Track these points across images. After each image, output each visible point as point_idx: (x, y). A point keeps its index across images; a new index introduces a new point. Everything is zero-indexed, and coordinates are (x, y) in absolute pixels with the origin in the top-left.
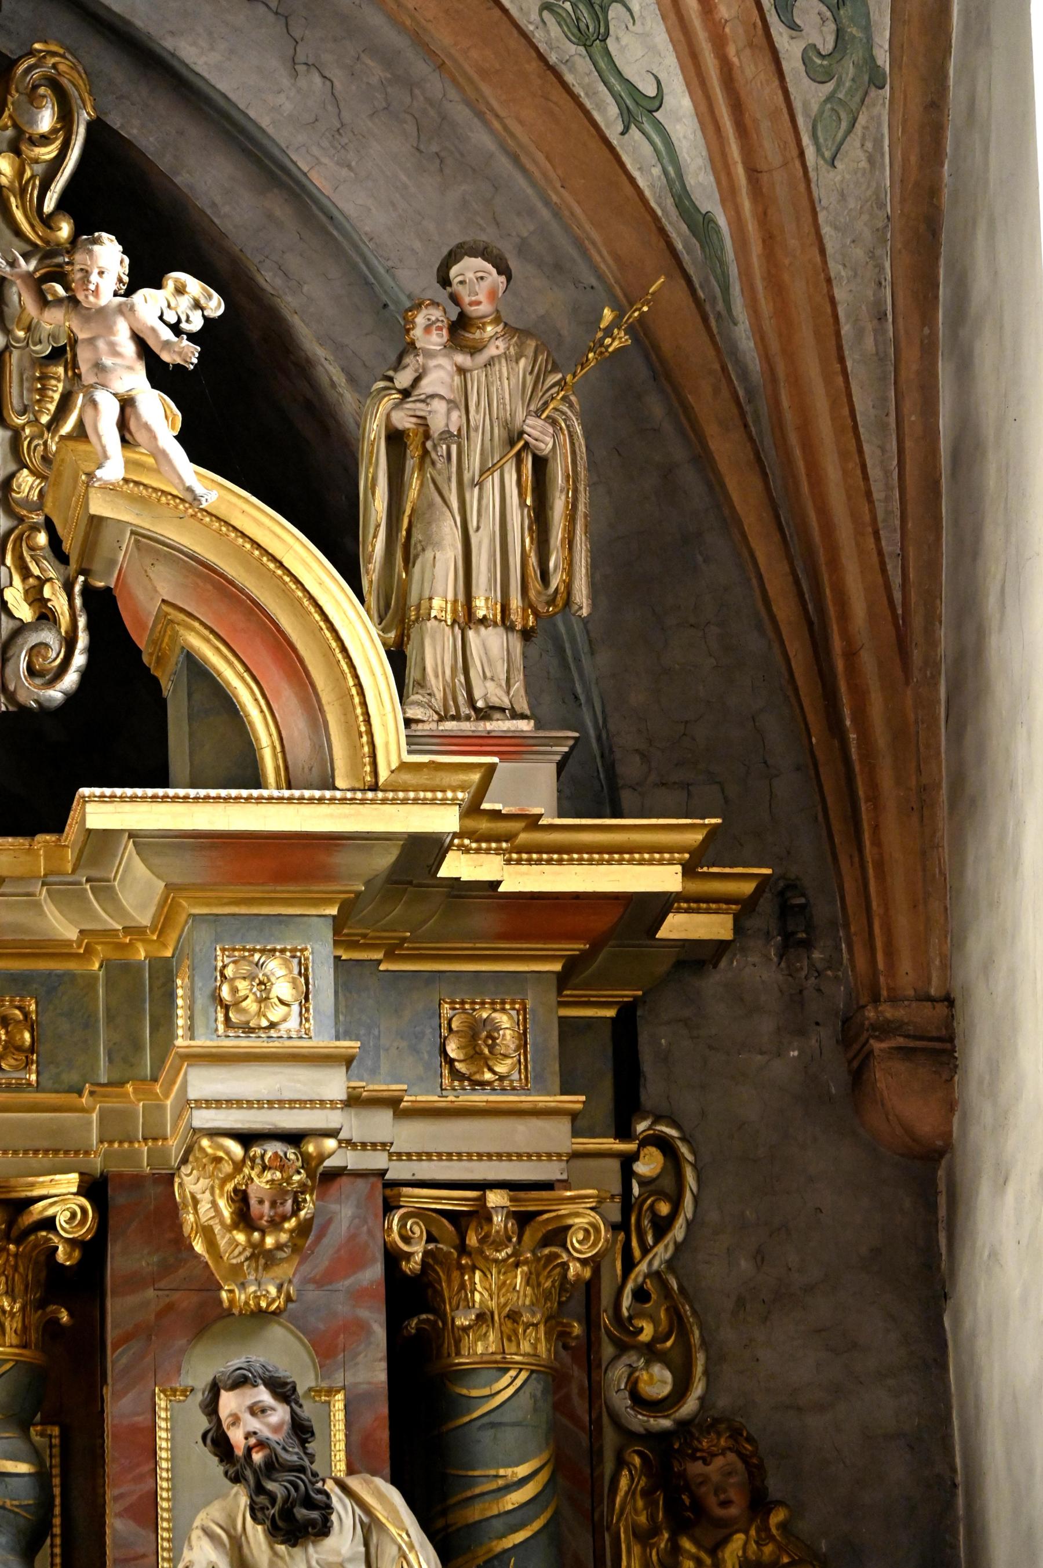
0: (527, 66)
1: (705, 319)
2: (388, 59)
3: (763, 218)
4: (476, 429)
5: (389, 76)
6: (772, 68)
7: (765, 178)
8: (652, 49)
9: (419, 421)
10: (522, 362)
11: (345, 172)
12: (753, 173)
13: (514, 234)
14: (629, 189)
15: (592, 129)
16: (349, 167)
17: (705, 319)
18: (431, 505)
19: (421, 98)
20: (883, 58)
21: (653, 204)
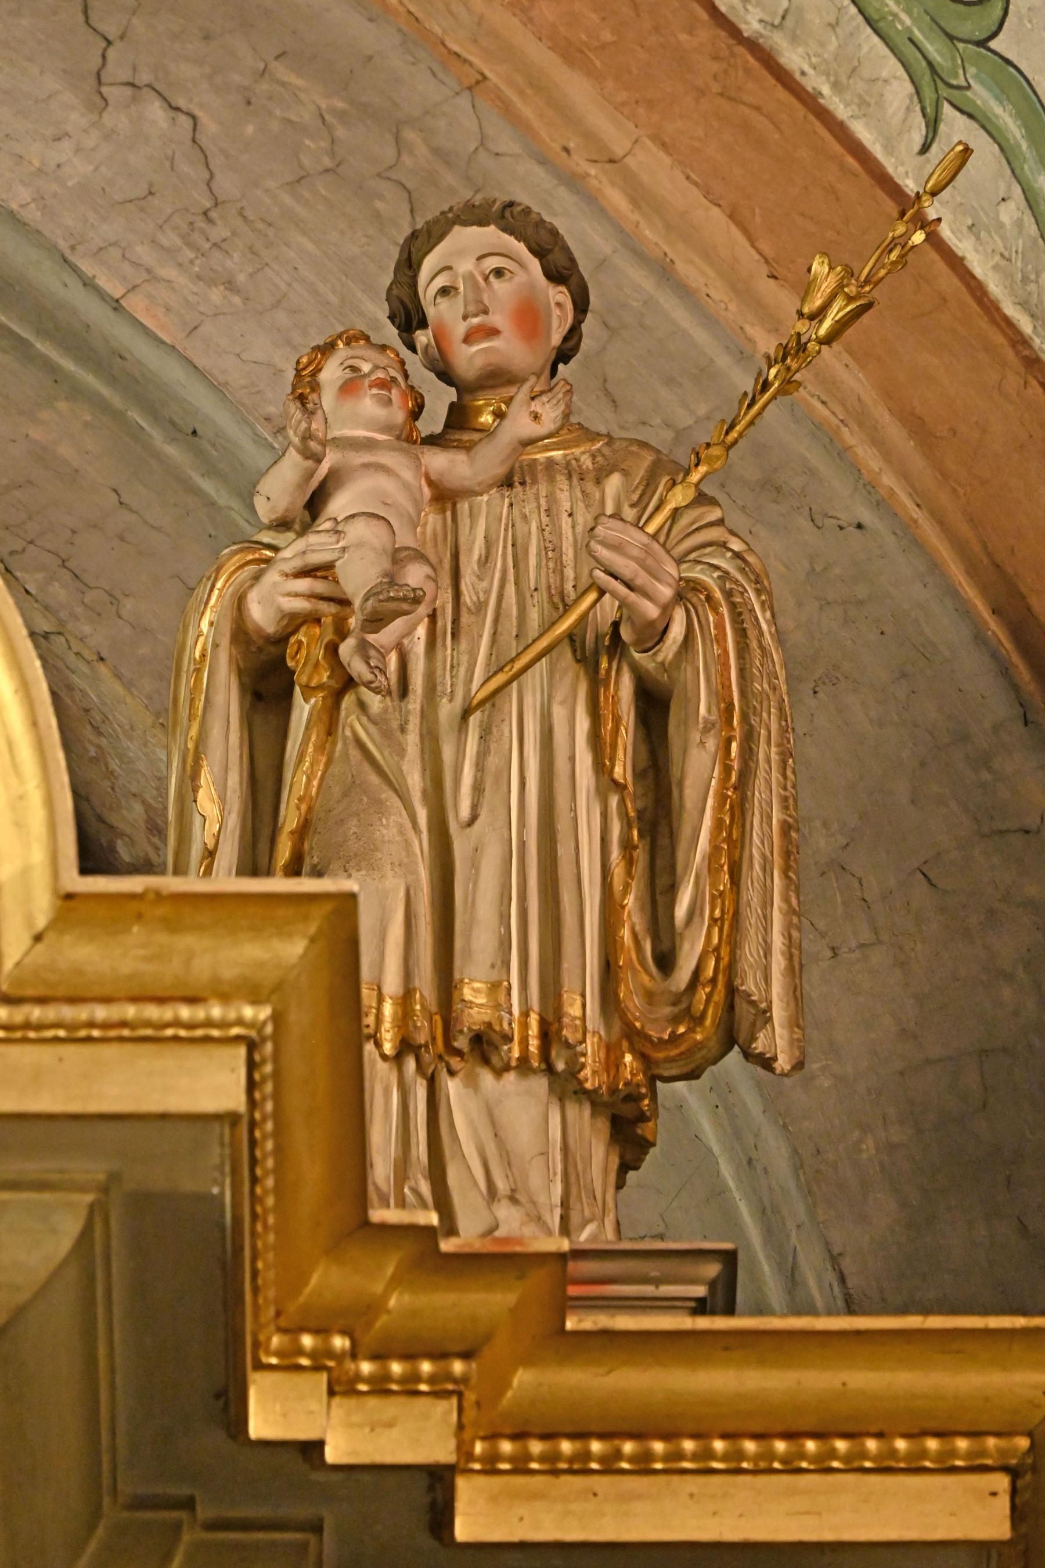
0: (683, 37)
4: (480, 607)
5: (340, 105)
9: (319, 586)
10: (614, 483)
11: (216, 295)
13: (657, 421)
14: (948, 281)
15: (850, 161)
16: (230, 285)
18: (353, 787)
19: (422, 150)
21: (1010, 310)
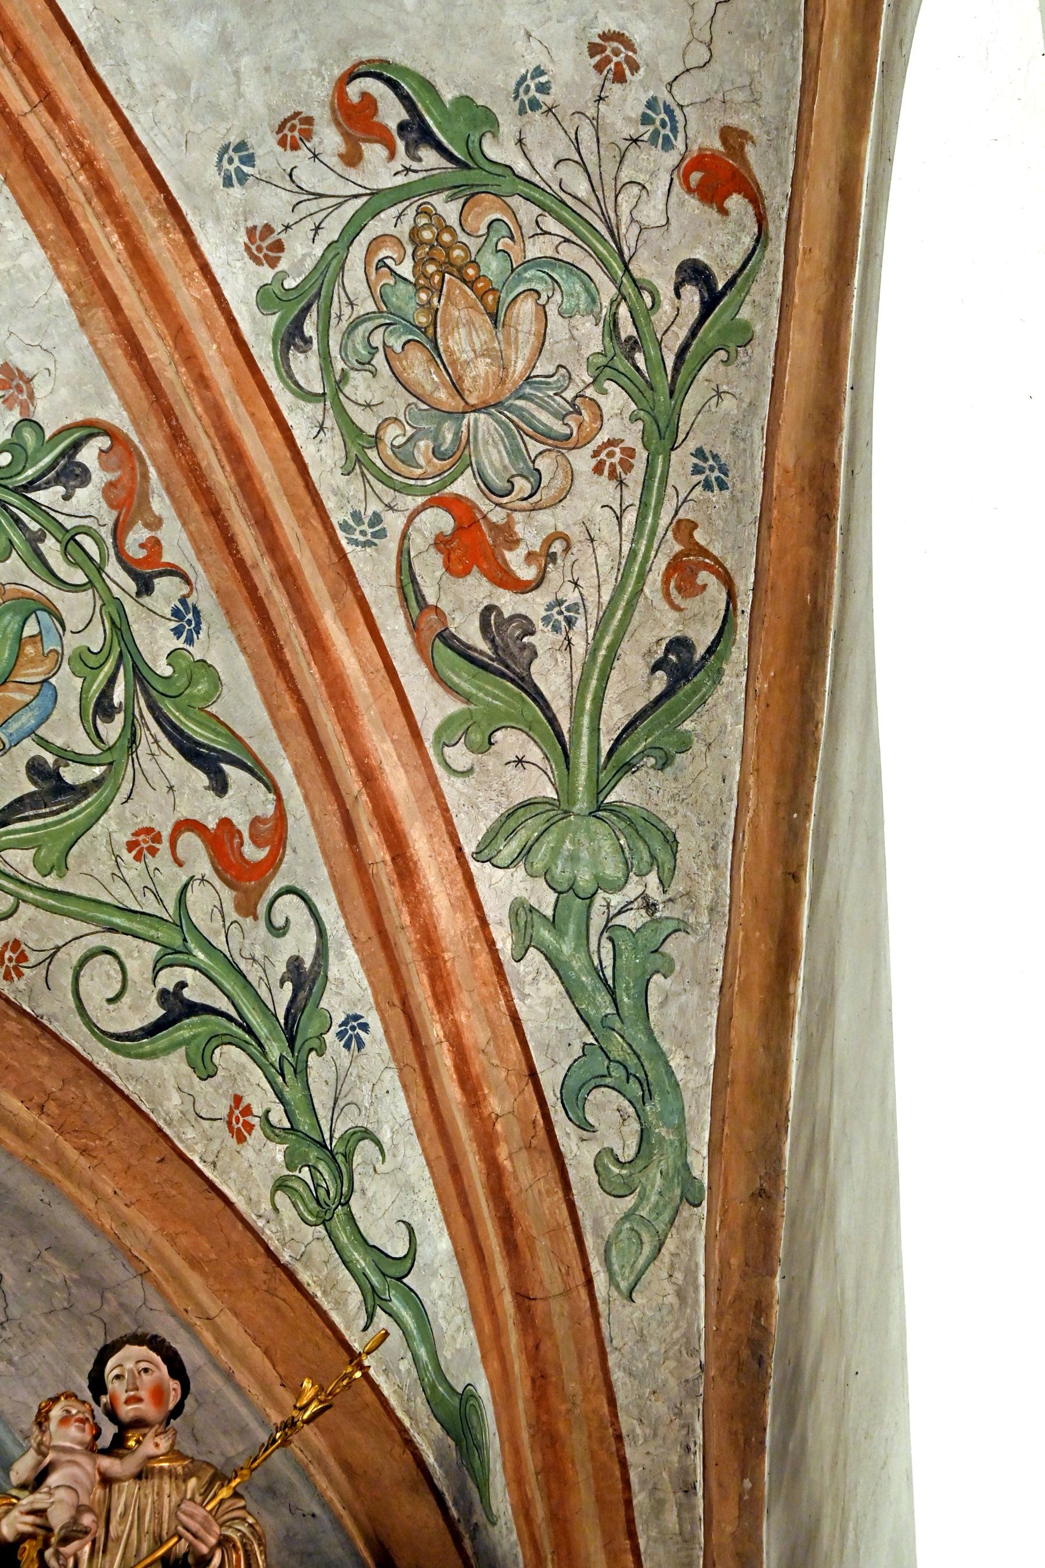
0: (251, 1260)
1: (457, 1539)
2: (79, 1261)
3: (534, 1354)
4: (119, 1539)
5: (75, 1276)
6: (554, 1175)
7: (539, 1307)
8: (409, 1188)
9: (38, 1520)
10: (193, 1482)
12: (523, 1298)
13: (217, 1452)
14: (370, 1396)
15: (327, 1330)
16: (10, 1362)
17: (457, 1539)
19: (114, 1303)
20: (700, 1167)
21: (400, 1414)
